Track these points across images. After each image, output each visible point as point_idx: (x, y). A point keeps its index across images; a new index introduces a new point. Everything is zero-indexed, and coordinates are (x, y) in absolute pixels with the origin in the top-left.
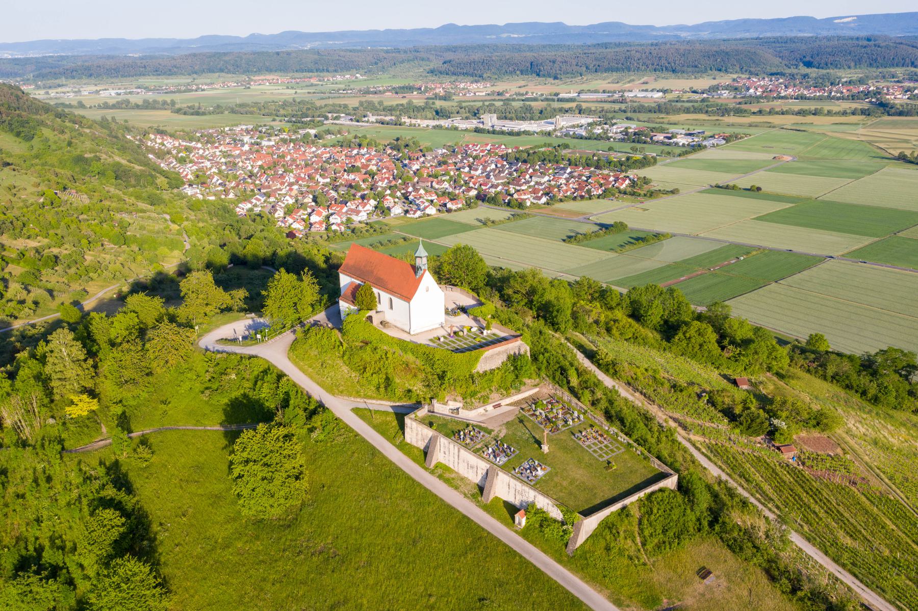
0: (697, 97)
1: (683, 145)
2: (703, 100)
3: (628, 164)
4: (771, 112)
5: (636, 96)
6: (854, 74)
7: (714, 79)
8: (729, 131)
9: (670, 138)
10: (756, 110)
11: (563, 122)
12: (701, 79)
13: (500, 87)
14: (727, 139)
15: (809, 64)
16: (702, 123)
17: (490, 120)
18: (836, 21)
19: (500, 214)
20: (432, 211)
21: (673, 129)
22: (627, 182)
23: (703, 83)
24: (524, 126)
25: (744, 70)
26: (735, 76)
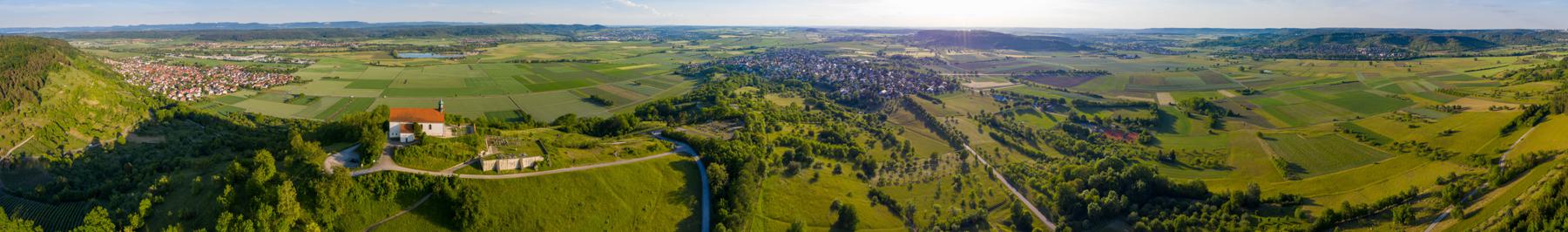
3: (288, 72)
4: (323, 52)
8: (315, 58)
11: (256, 56)
13: (224, 44)
14: (316, 61)
17: (228, 56)
19: (254, 93)
20: (225, 92)
24: (242, 58)
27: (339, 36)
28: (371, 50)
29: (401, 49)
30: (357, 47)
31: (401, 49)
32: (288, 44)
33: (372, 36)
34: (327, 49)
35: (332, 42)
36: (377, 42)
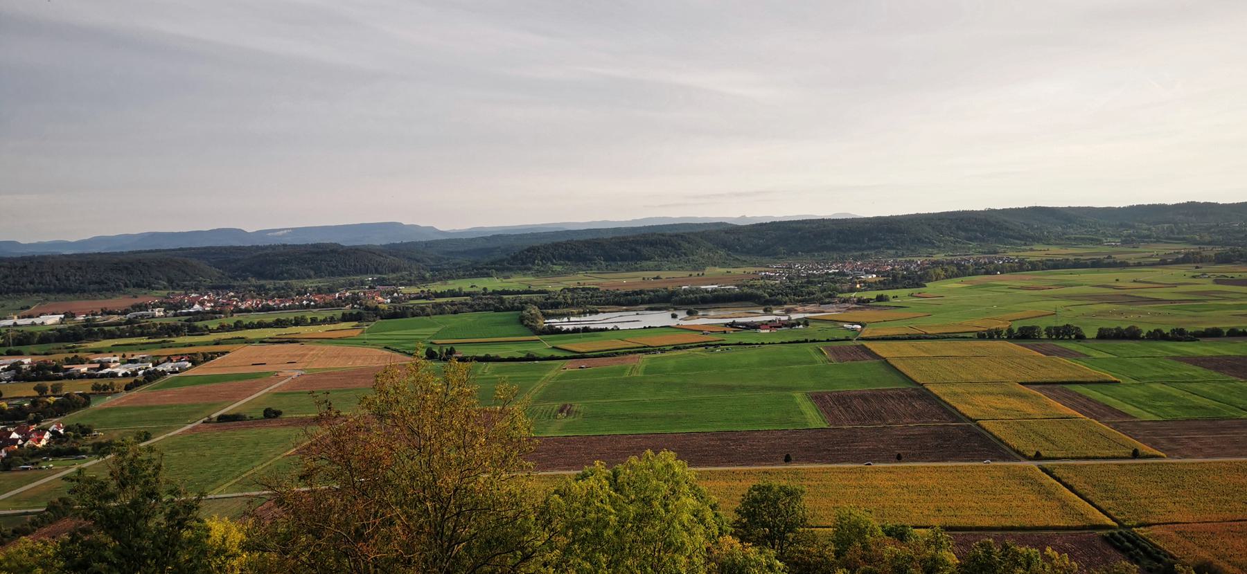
0: (115, 318)
1: (125, 375)
2: (129, 322)
4: (238, 326)
5: (15, 324)
6: (323, 283)
7: (136, 297)
9: (102, 367)
10: (215, 327)
12: (114, 299)
15: (260, 275)
16: (141, 347)
18: (269, 234)
21: (106, 358)
22: (47, 435)
23: (120, 302)
25: (174, 284)
26: (165, 293)
27: (318, 273)
28: (440, 310)
29: (552, 305)
30: (384, 302)
31: (552, 305)
32: (84, 310)
33: (440, 274)
34: (255, 318)
35: (283, 294)
36: (465, 285)
